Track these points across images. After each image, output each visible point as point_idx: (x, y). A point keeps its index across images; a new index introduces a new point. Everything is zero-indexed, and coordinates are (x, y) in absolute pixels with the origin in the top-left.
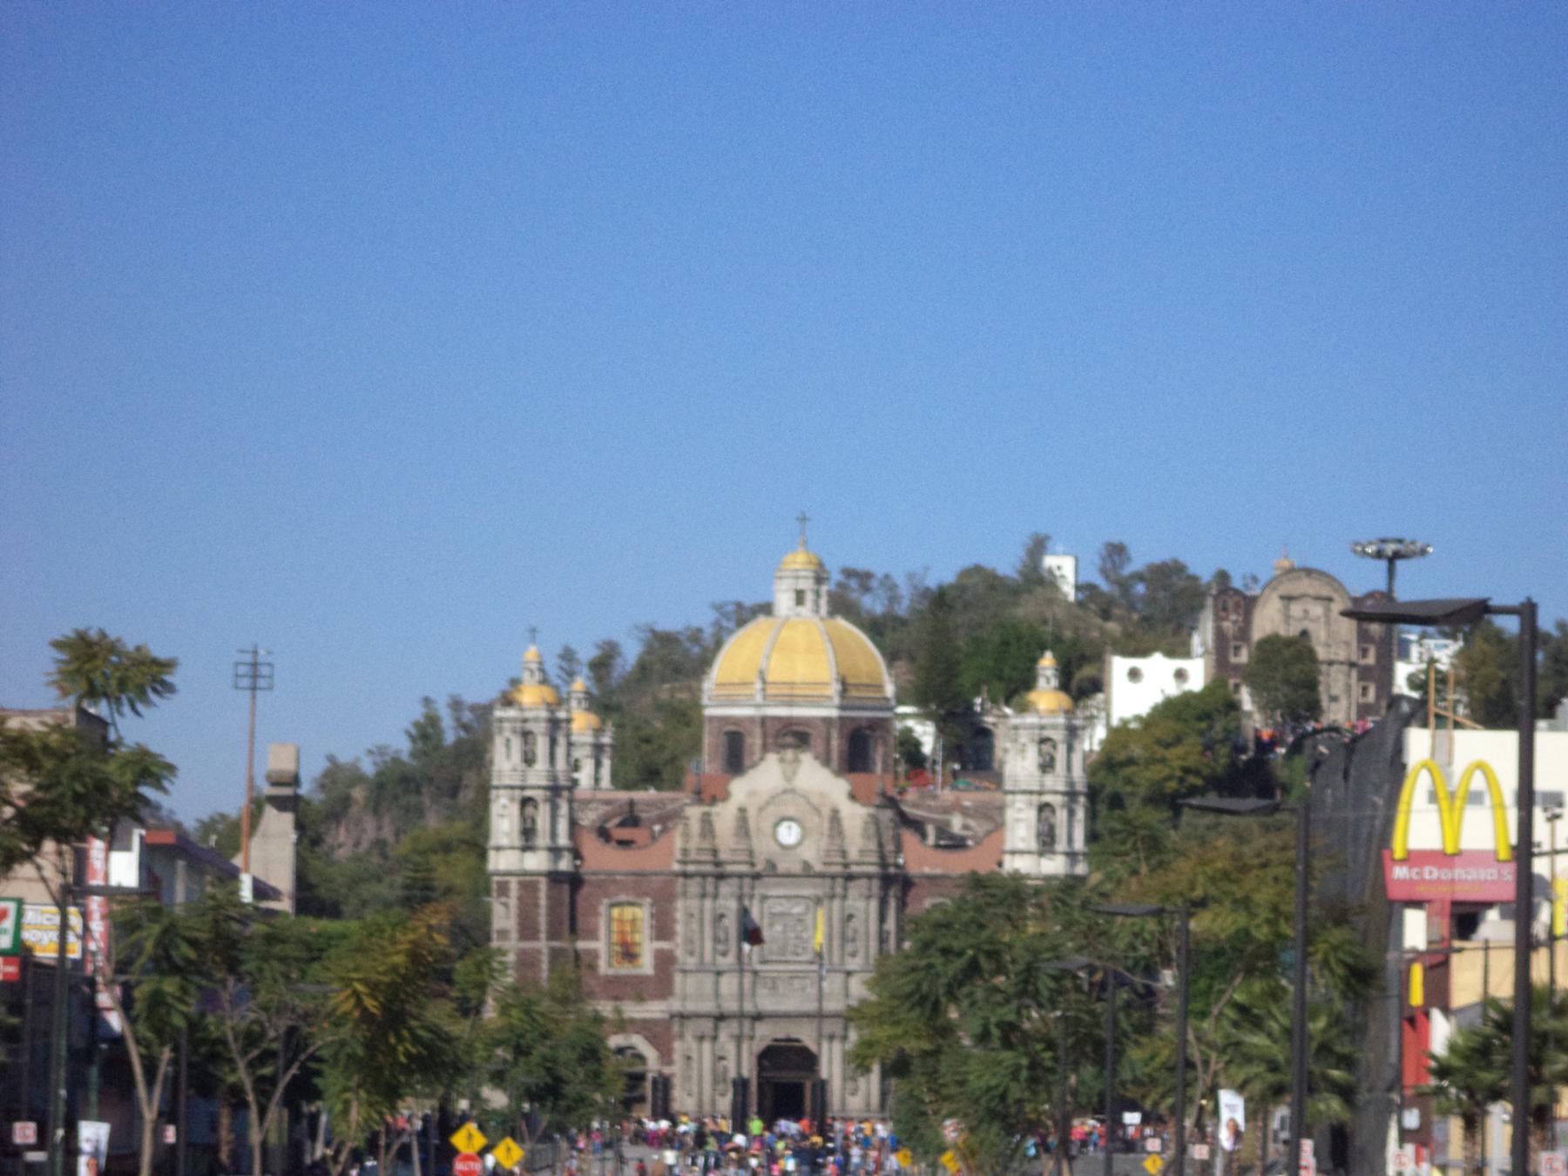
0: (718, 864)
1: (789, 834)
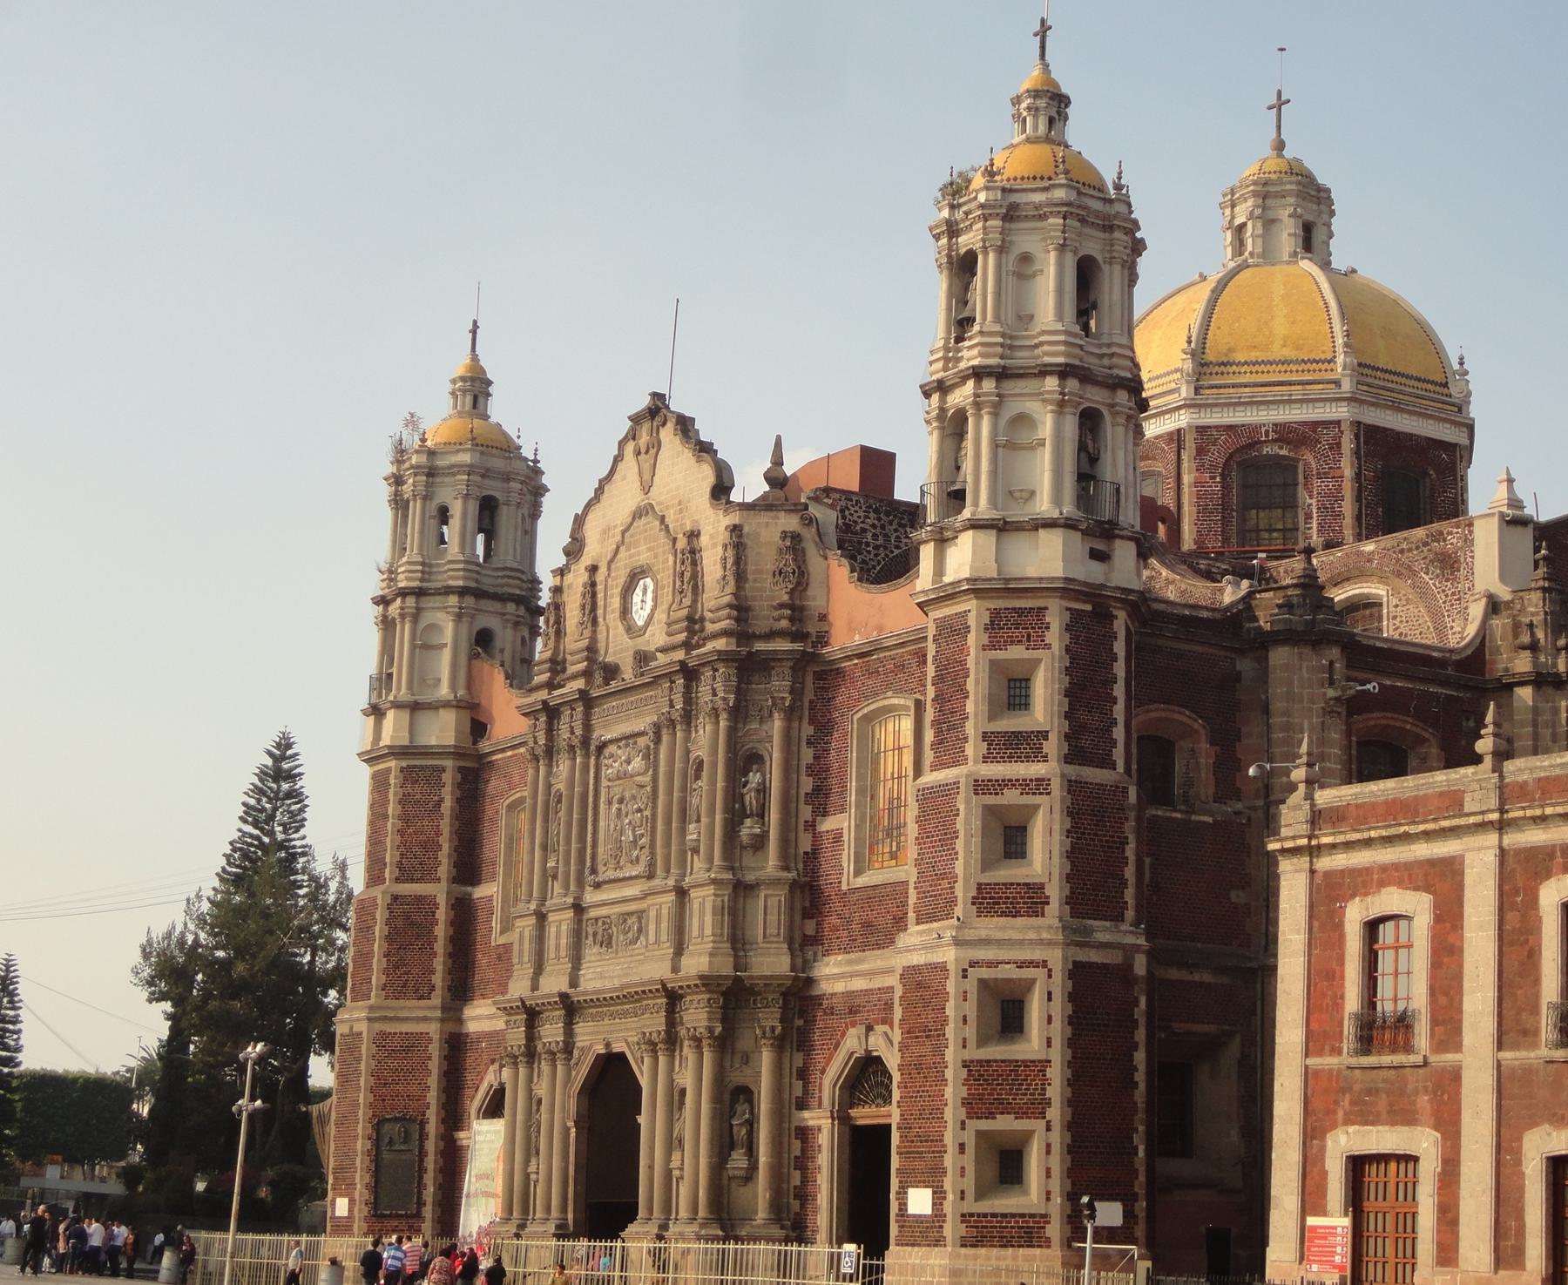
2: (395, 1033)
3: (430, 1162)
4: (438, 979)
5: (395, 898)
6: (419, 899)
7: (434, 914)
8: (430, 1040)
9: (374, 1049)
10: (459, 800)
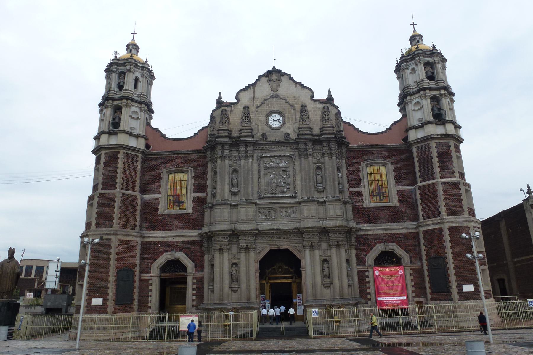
0: (231, 138)
1: (275, 121)
2: (125, 240)
3: (137, 285)
4: (138, 223)
5: (123, 194)
6: (132, 196)
7: (136, 201)
8: (137, 243)
9: (117, 245)
10: (141, 167)
